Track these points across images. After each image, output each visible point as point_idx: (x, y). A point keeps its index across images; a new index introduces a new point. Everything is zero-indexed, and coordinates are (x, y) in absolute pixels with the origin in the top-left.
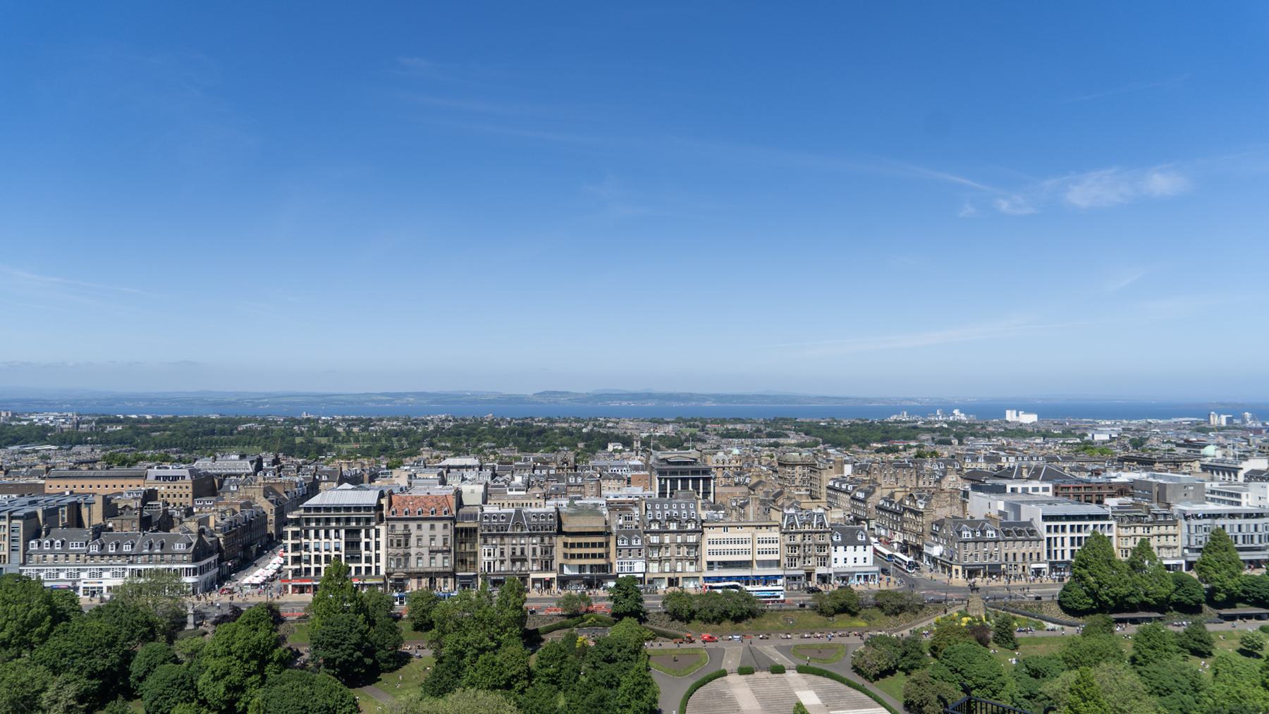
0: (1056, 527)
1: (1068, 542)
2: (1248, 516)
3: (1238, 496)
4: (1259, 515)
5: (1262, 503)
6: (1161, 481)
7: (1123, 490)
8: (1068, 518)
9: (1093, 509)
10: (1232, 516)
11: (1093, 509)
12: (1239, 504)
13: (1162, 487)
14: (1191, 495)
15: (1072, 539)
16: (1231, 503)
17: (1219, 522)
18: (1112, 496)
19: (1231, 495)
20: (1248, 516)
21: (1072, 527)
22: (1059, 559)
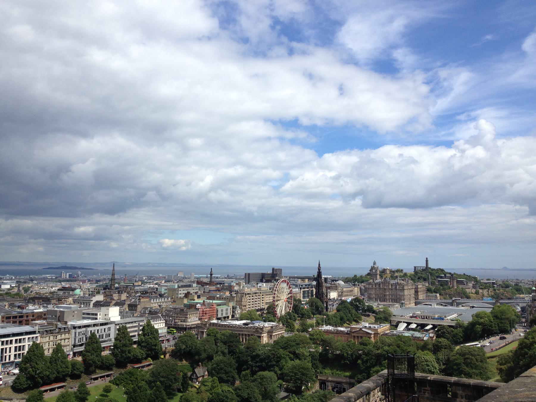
0: (7, 341)
1: (13, 350)
2: (102, 324)
3: (96, 315)
4: (106, 324)
5: (106, 317)
6: (62, 310)
7: (40, 316)
8: (14, 335)
9: (27, 328)
10: (94, 325)
11: (27, 328)
12: (96, 319)
13: (62, 313)
14: (75, 316)
15: (16, 347)
16: (93, 319)
17: (89, 329)
18: (32, 320)
19: (93, 314)
20: (102, 324)
21: (16, 340)
22: (7, 361)
